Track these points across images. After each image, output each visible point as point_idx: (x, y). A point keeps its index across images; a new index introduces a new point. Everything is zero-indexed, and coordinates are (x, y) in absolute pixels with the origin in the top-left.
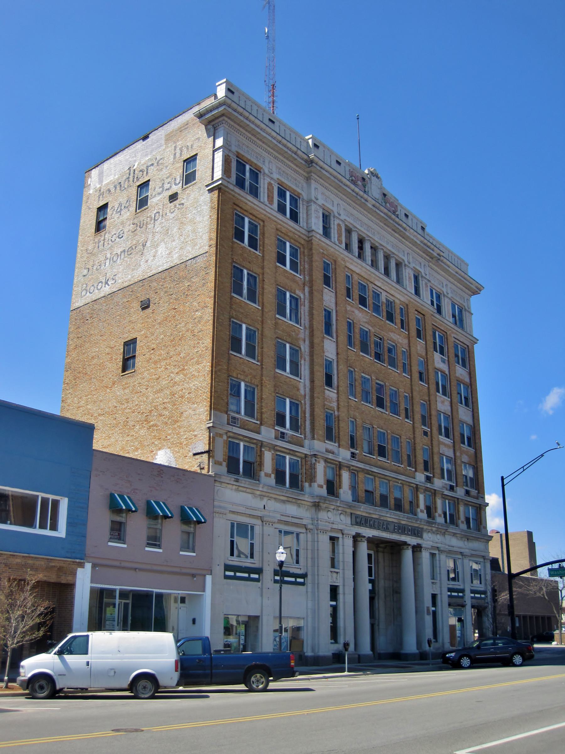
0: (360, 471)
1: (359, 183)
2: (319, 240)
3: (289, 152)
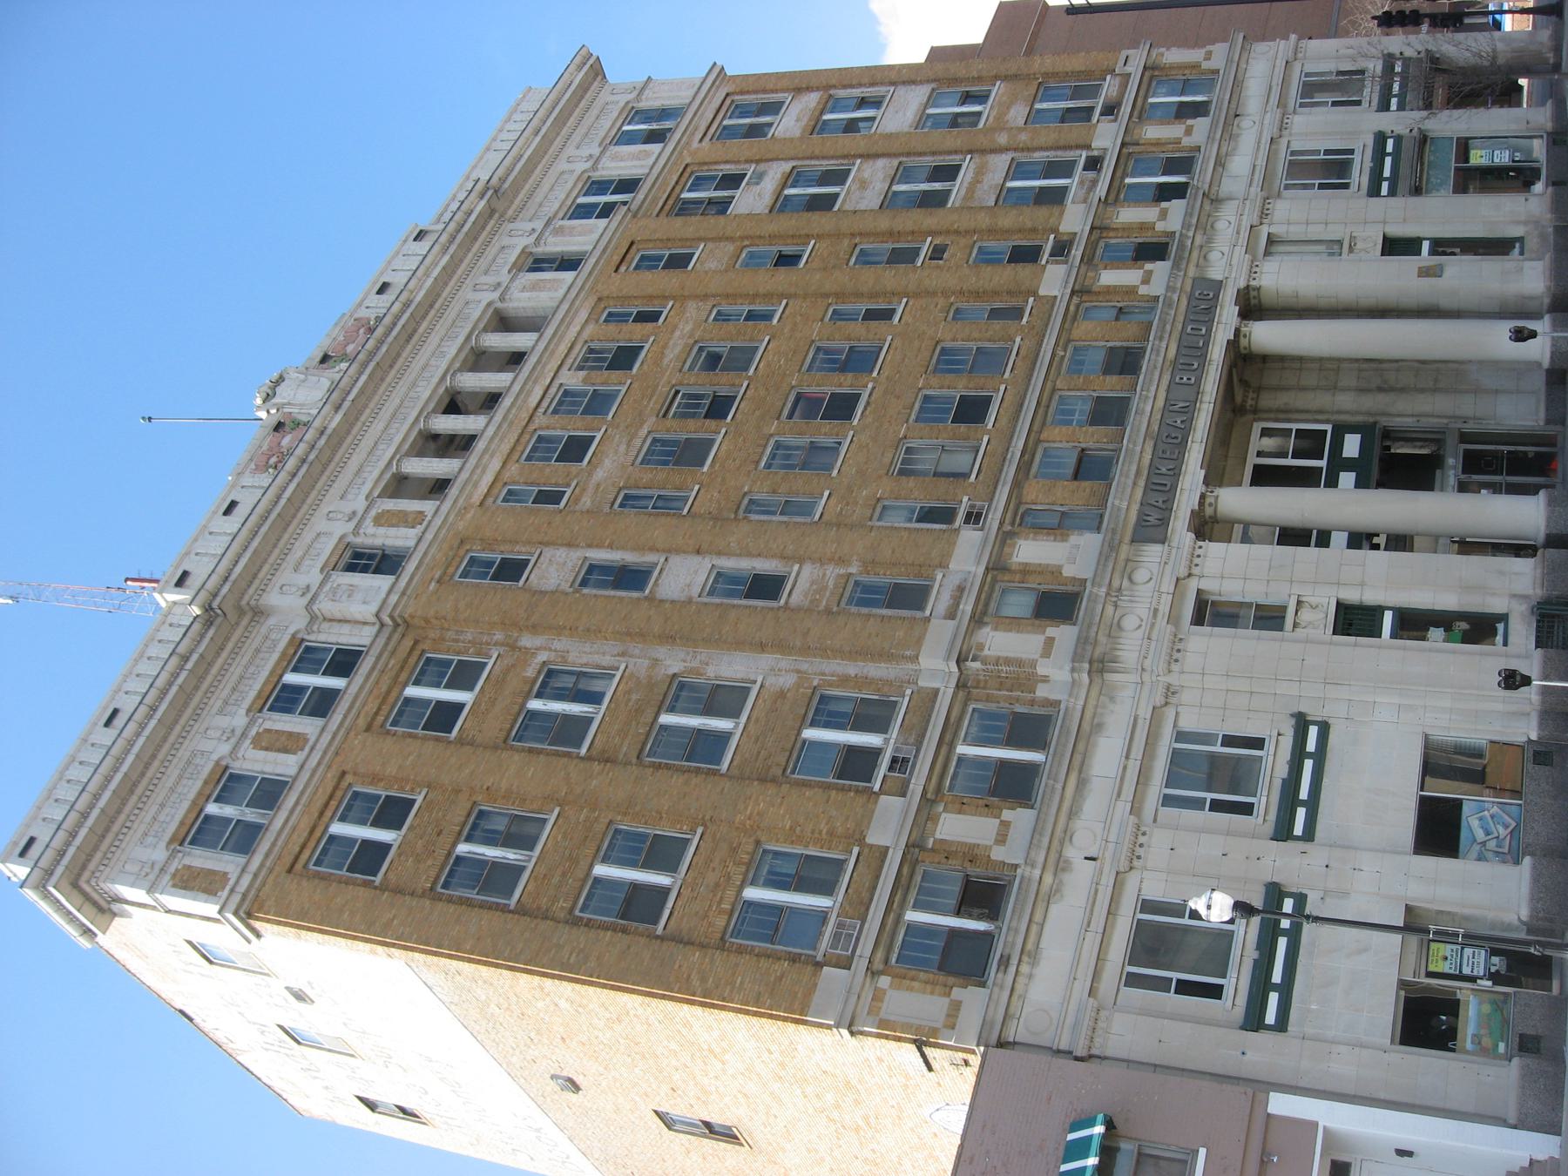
0: (1020, 496)
1: (286, 441)
2: (403, 594)
3: (180, 680)
